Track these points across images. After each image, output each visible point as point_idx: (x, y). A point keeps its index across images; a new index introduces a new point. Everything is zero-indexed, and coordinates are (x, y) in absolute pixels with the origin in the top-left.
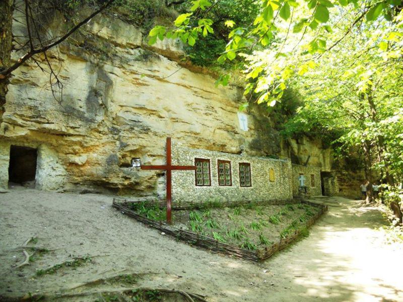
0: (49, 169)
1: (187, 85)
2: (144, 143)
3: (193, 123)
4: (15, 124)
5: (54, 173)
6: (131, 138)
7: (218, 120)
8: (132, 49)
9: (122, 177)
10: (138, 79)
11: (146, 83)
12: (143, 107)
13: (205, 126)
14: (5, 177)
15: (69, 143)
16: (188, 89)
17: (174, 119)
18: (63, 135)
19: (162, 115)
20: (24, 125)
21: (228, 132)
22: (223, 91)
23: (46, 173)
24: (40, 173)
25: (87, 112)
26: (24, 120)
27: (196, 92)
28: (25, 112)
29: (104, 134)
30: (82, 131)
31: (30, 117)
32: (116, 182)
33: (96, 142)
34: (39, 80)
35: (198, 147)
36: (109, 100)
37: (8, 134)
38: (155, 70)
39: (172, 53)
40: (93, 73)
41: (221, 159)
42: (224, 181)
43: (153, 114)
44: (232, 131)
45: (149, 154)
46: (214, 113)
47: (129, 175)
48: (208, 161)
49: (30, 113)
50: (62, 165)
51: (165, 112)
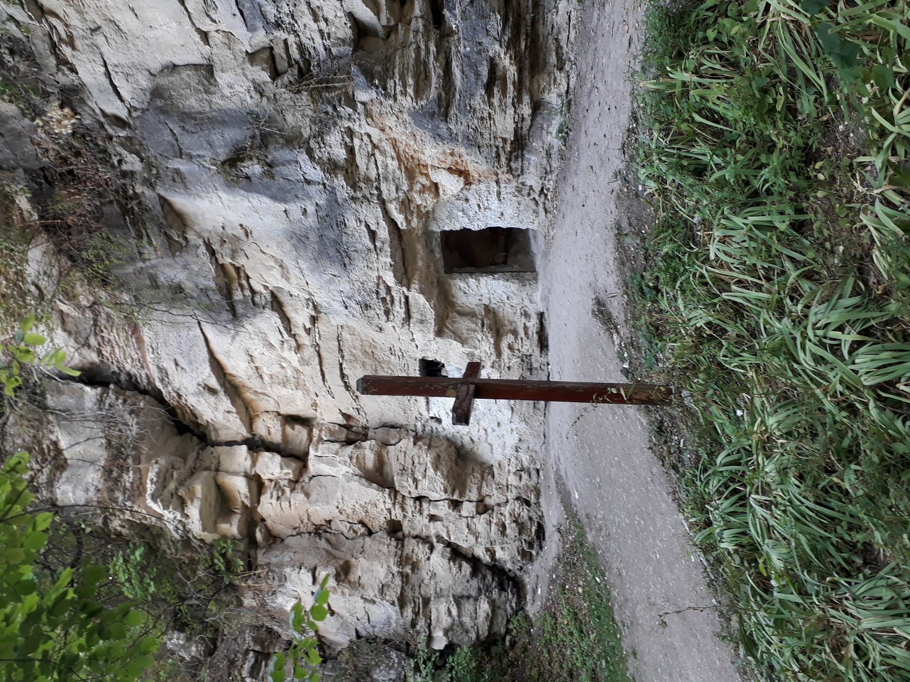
9: (489, 93)
20: (403, 300)
33: (383, 153)
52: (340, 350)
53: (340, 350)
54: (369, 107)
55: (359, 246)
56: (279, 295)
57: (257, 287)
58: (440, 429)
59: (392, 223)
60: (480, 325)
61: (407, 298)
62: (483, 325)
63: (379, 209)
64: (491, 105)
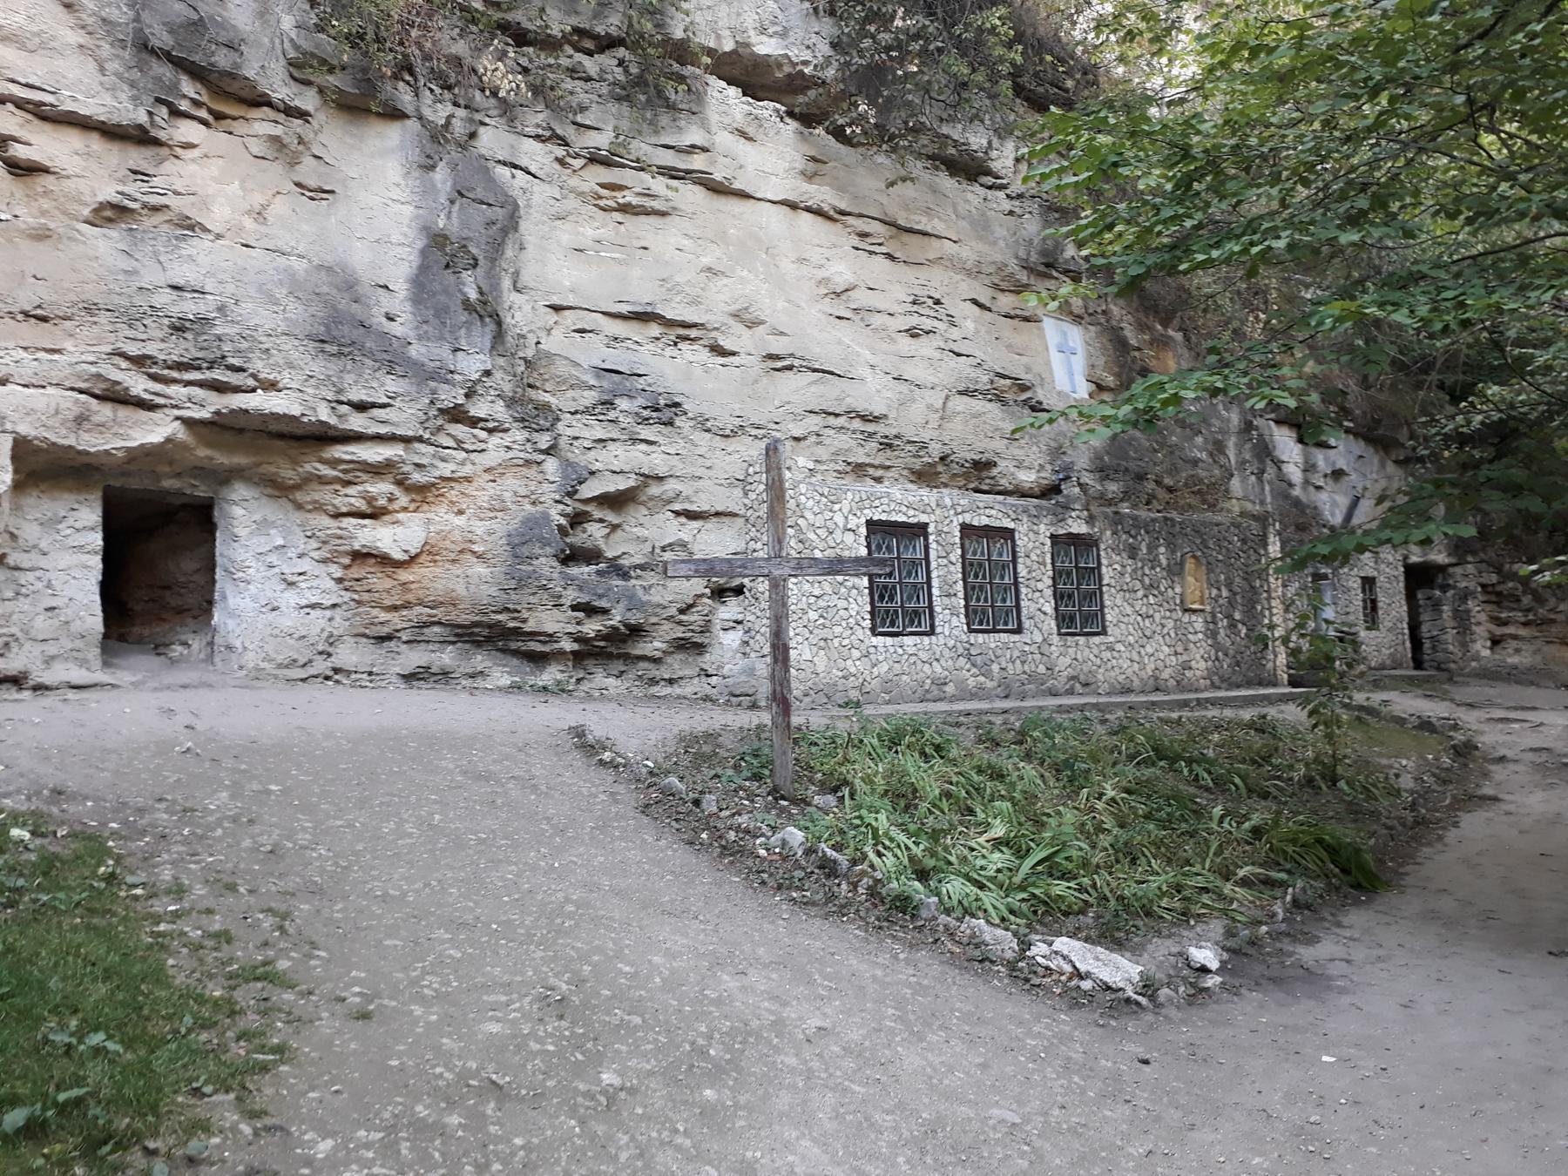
0: (268, 570)
1: (826, 208)
2: (656, 461)
3: (865, 372)
4: (116, 397)
5: (290, 598)
7: (959, 355)
8: (590, 53)
9: (574, 608)
10: (620, 188)
11: (656, 205)
12: (649, 309)
13: (904, 387)
14: (90, 620)
15: (345, 471)
16: (828, 225)
17: (778, 357)
18: (325, 437)
19: (726, 343)
20: (161, 401)
21: (1004, 403)
22: (981, 226)
24: (233, 601)
25: (420, 338)
26: (155, 378)
27: (863, 235)
28: (163, 346)
29: (490, 431)
30: (404, 418)
31: (180, 366)
32: (550, 628)
33: (462, 463)
34: (205, 205)
35: (879, 473)
36: (506, 283)
38: (693, 146)
39: (763, 64)
40: (433, 167)
41: (975, 523)
42: (992, 606)
43: (687, 338)
44: (1017, 393)
45: (677, 507)
46: (941, 326)
48: (923, 527)
49: (178, 349)
51: (739, 328)
54: (535, 467)
55: (349, 378)
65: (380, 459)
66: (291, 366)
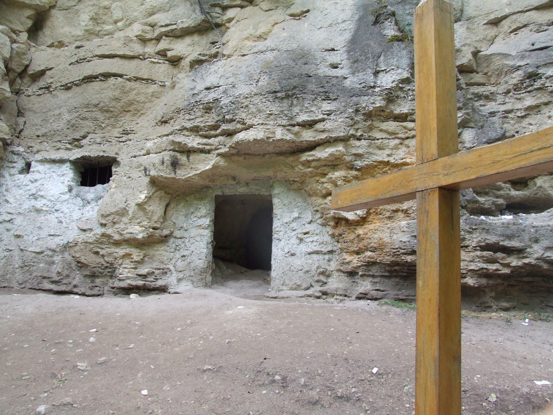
4: (188, 152)
6: (535, 109)
18: (300, 149)
20: (208, 147)
23: (283, 250)
25: (353, 74)
26: (206, 137)
28: (201, 119)
30: (336, 126)
31: (215, 127)
33: (396, 148)
37: (182, 174)
47: (510, 237)
49: (211, 119)
50: (324, 225)
52: (137, 79)
53: (137, 79)
55: (296, 110)
56: (217, 31)
57: (231, 13)
58: (13, 171)
59: (312, 146)
60: (155, 225)
61: (209, 152)
62: (154, 228)
63: (342, 134)
64: (475, 249)
65: (326, 155)
66: (260, 111)
